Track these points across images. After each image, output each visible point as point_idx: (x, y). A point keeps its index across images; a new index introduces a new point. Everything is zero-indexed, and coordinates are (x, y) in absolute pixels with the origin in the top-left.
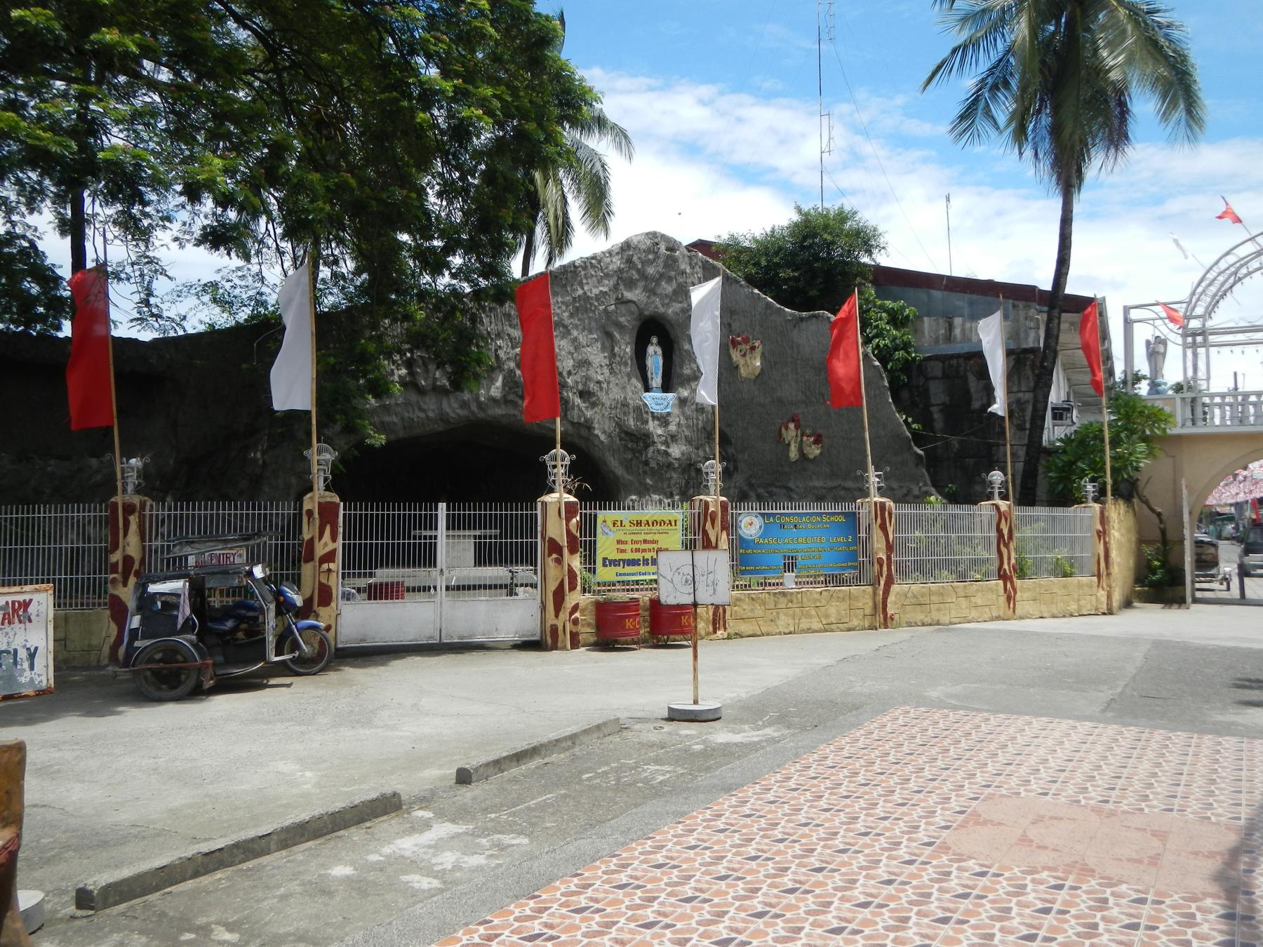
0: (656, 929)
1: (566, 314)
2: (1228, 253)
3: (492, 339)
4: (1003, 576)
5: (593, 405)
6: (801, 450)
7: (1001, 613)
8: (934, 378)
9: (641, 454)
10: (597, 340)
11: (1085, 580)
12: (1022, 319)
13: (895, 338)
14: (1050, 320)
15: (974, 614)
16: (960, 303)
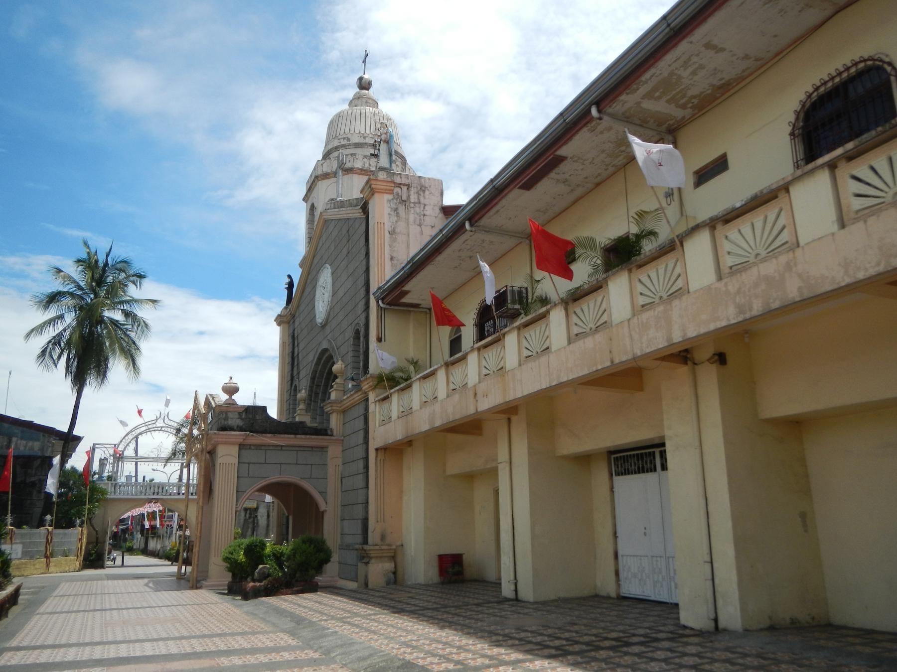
4: (46, 557)
11: (72, 558)
15: (35, 572)
16: (16, 431)
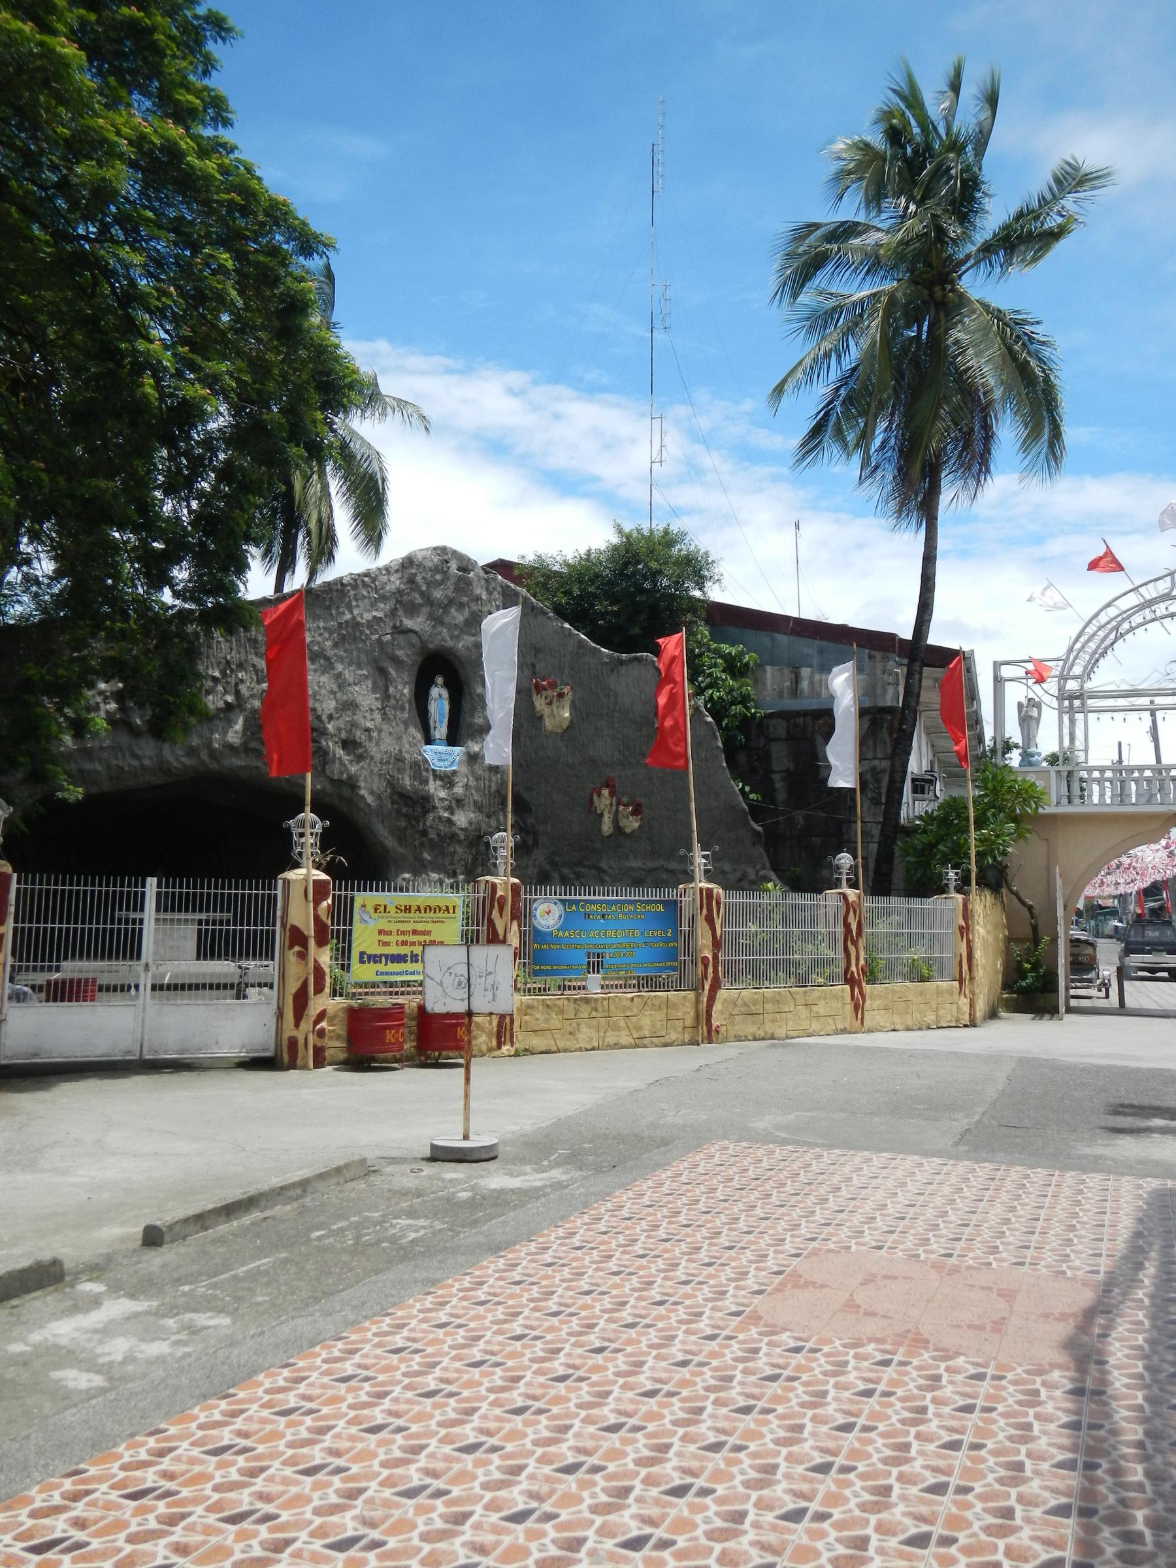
0: (384, 1434)
1: (329, 644)
2: (1108, 605)
3: (232, 670)
4: (850, 980)
5: (360, 758)
6: (615, 821)
7: (847, 1025)
8: (778, 739)
9: (418, 821)
10: (366, 677)
12: (878, 672)
13: (731, 690)
14: (909, 676)
15: (815, 1026)
